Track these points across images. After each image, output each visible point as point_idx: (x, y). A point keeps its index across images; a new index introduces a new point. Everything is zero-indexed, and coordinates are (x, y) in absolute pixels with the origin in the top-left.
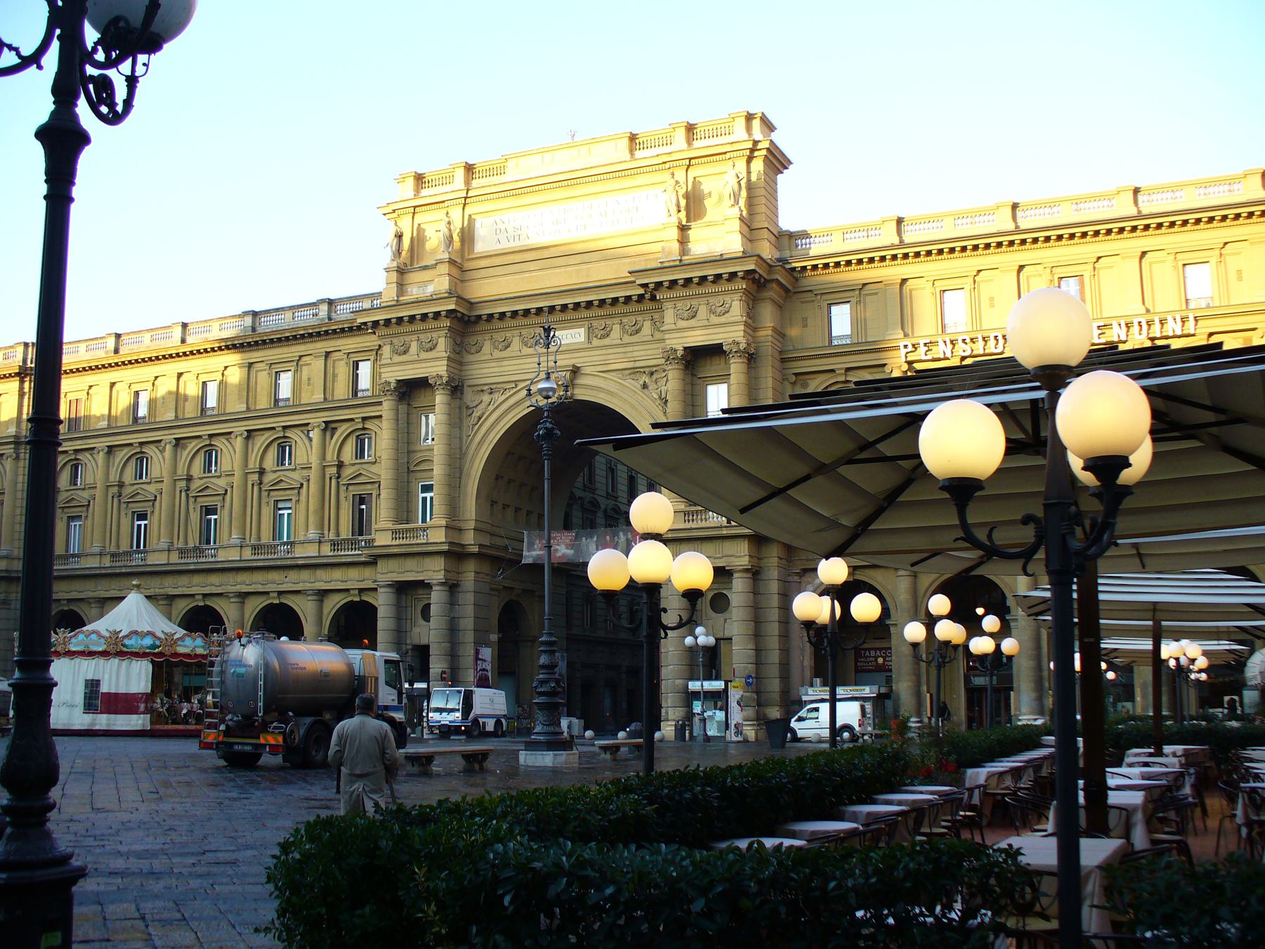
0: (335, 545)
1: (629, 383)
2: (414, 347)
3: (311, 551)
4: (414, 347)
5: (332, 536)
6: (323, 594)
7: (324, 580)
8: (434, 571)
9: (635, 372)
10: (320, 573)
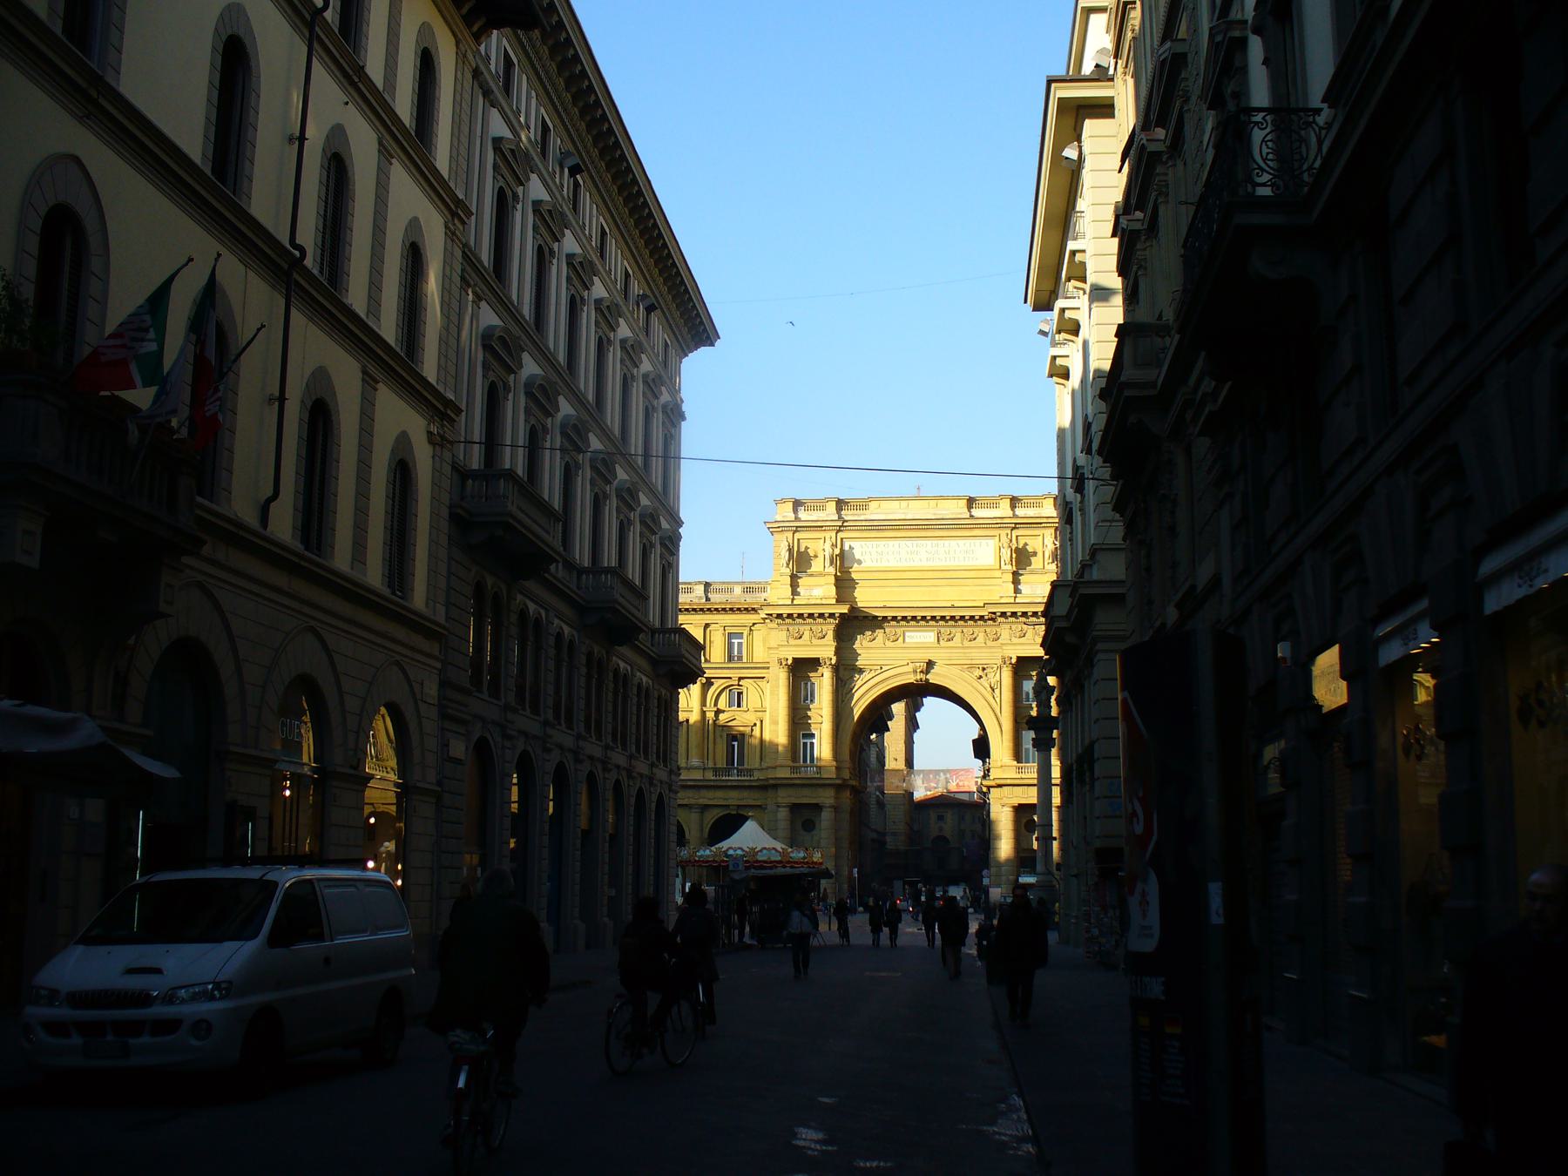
0: (716, 770)
1: (966, 675)
2: (807, 634)
3: (697, 775)
4: (807, 634)
5: (711, 765)
6: (706, 807)
7: (706, 798)
8: (826, 798)
9: (971, 667)
10: (704, 793)
